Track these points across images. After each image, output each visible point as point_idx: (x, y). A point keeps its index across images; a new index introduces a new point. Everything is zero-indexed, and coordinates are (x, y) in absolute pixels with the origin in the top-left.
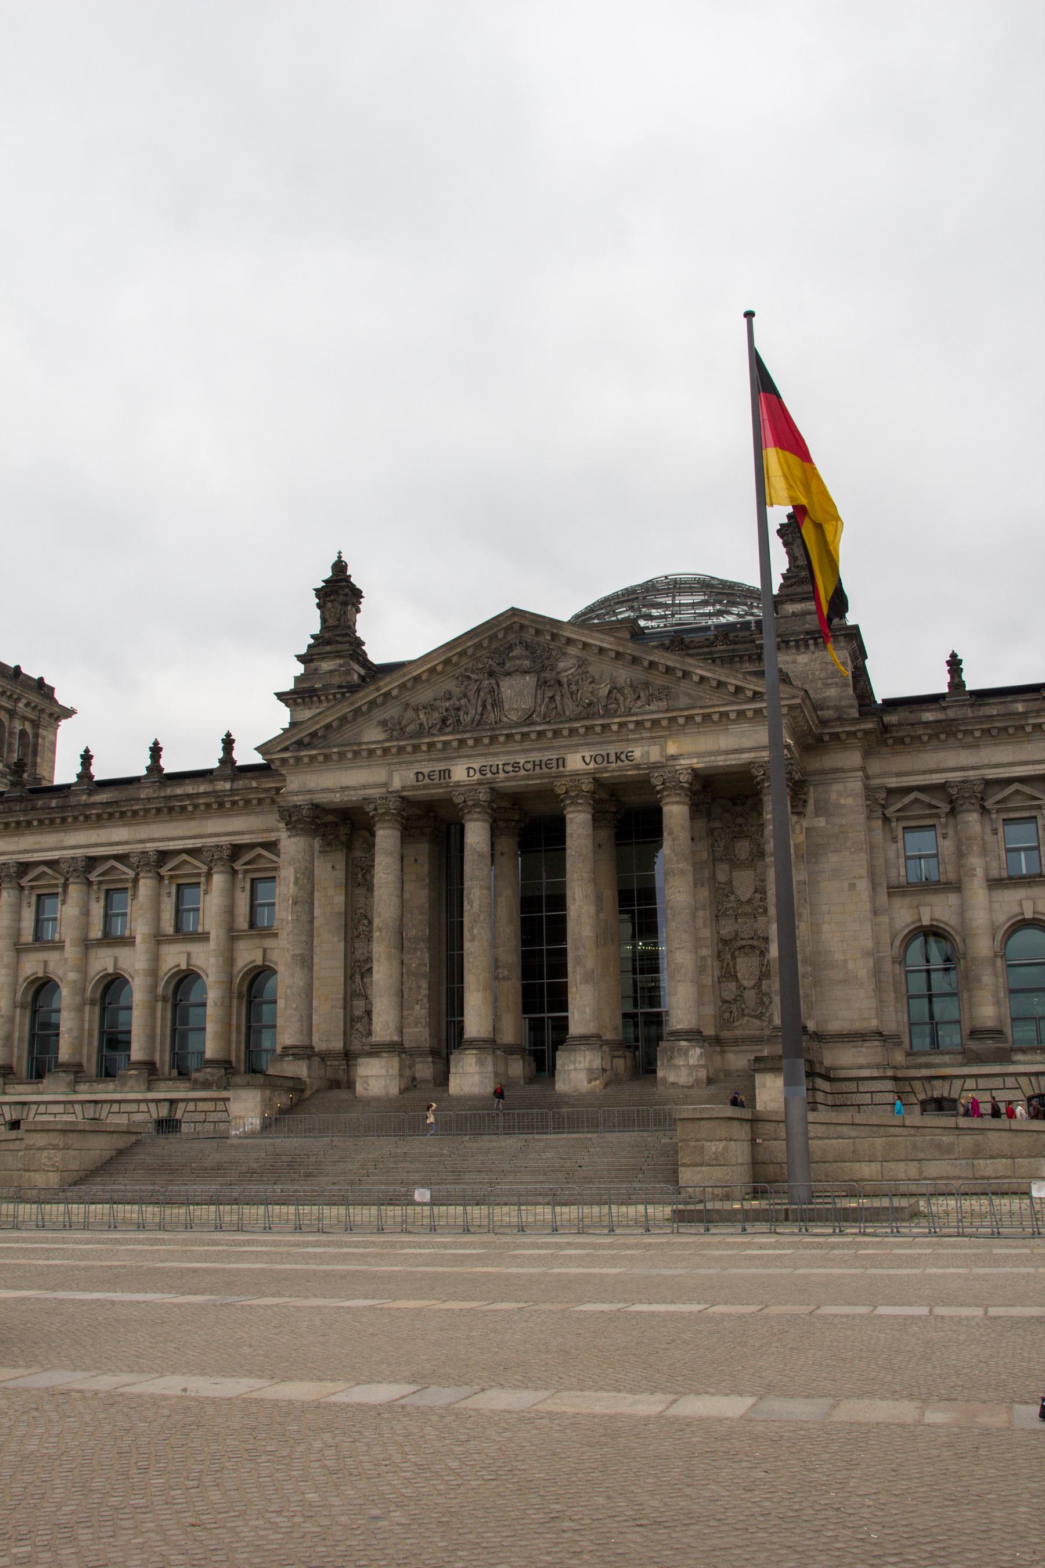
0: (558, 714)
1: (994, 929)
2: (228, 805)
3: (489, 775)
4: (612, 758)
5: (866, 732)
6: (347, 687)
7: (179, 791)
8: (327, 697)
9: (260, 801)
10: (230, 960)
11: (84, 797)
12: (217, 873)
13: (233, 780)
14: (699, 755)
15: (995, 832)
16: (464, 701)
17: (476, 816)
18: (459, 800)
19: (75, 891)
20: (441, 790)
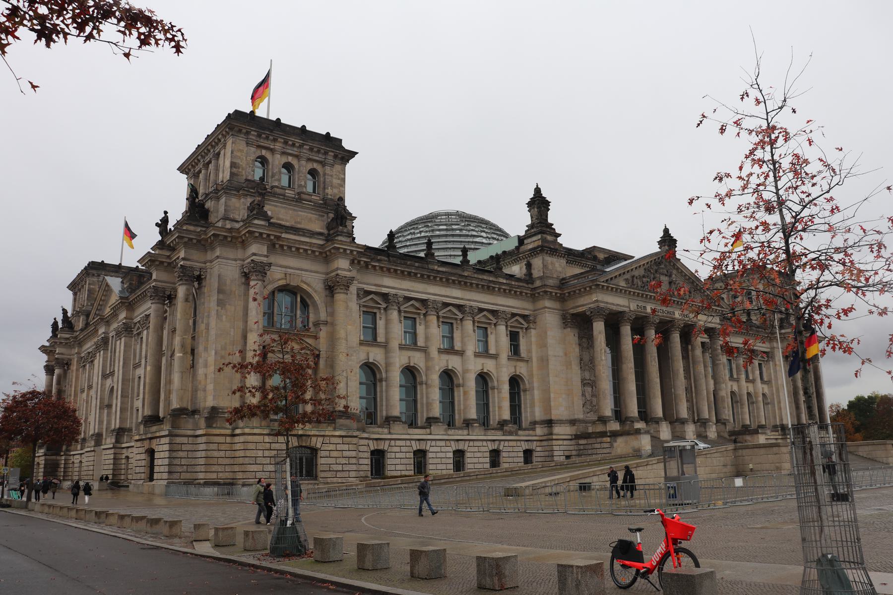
2: (513, 292)
6: (569, 253)
7: (480, 277)
12: (503, 325)
13: (507, 279)
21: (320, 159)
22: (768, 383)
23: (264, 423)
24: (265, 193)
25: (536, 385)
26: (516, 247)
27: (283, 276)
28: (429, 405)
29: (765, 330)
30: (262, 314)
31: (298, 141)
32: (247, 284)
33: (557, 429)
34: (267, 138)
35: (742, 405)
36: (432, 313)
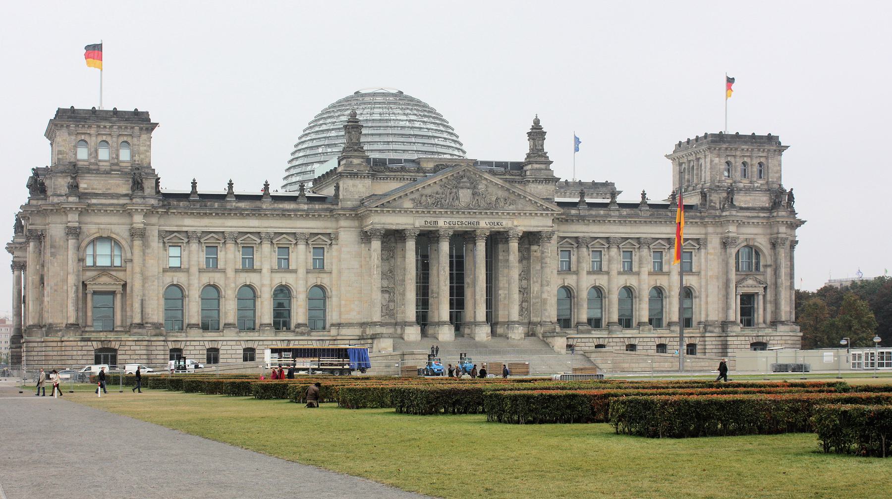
0: (479, 206)
1: (587, 288)
2: (310, 216)
3: (452, 225)
4: (496, 224)
5: (562, 218)
8: (361, 178)
9: (325, 215)
10: (307, 282)
11: (234, 204)
14: (525, 226)
15: (589, 255)
16: (444, 196)
17: (447, 240)
18: (442, 233)
19: (231, 246)
20: (434, 229)
21: (129, 133)
22: (698, 274)
23: (77, 334)
24: (76, 176)
25: (334, 293)
26: (336, 168)
27: (97, 230)
28: (226, 313)
29: (701, 213)
30: (77, 261)
31: (108, 124)
32: (68, 240)
33: (344, 331)
34: (83, 126)
35: (640, 300)
36: (230, 242)
